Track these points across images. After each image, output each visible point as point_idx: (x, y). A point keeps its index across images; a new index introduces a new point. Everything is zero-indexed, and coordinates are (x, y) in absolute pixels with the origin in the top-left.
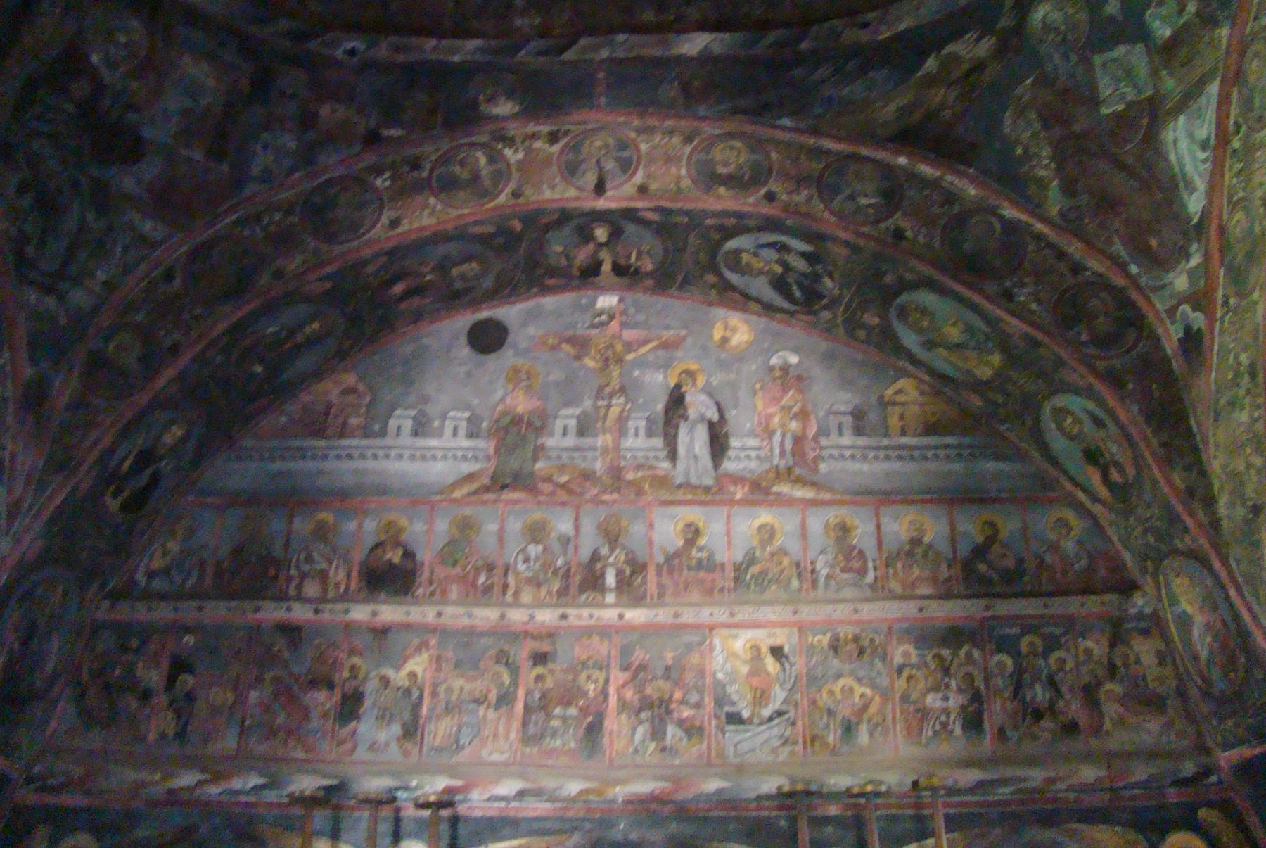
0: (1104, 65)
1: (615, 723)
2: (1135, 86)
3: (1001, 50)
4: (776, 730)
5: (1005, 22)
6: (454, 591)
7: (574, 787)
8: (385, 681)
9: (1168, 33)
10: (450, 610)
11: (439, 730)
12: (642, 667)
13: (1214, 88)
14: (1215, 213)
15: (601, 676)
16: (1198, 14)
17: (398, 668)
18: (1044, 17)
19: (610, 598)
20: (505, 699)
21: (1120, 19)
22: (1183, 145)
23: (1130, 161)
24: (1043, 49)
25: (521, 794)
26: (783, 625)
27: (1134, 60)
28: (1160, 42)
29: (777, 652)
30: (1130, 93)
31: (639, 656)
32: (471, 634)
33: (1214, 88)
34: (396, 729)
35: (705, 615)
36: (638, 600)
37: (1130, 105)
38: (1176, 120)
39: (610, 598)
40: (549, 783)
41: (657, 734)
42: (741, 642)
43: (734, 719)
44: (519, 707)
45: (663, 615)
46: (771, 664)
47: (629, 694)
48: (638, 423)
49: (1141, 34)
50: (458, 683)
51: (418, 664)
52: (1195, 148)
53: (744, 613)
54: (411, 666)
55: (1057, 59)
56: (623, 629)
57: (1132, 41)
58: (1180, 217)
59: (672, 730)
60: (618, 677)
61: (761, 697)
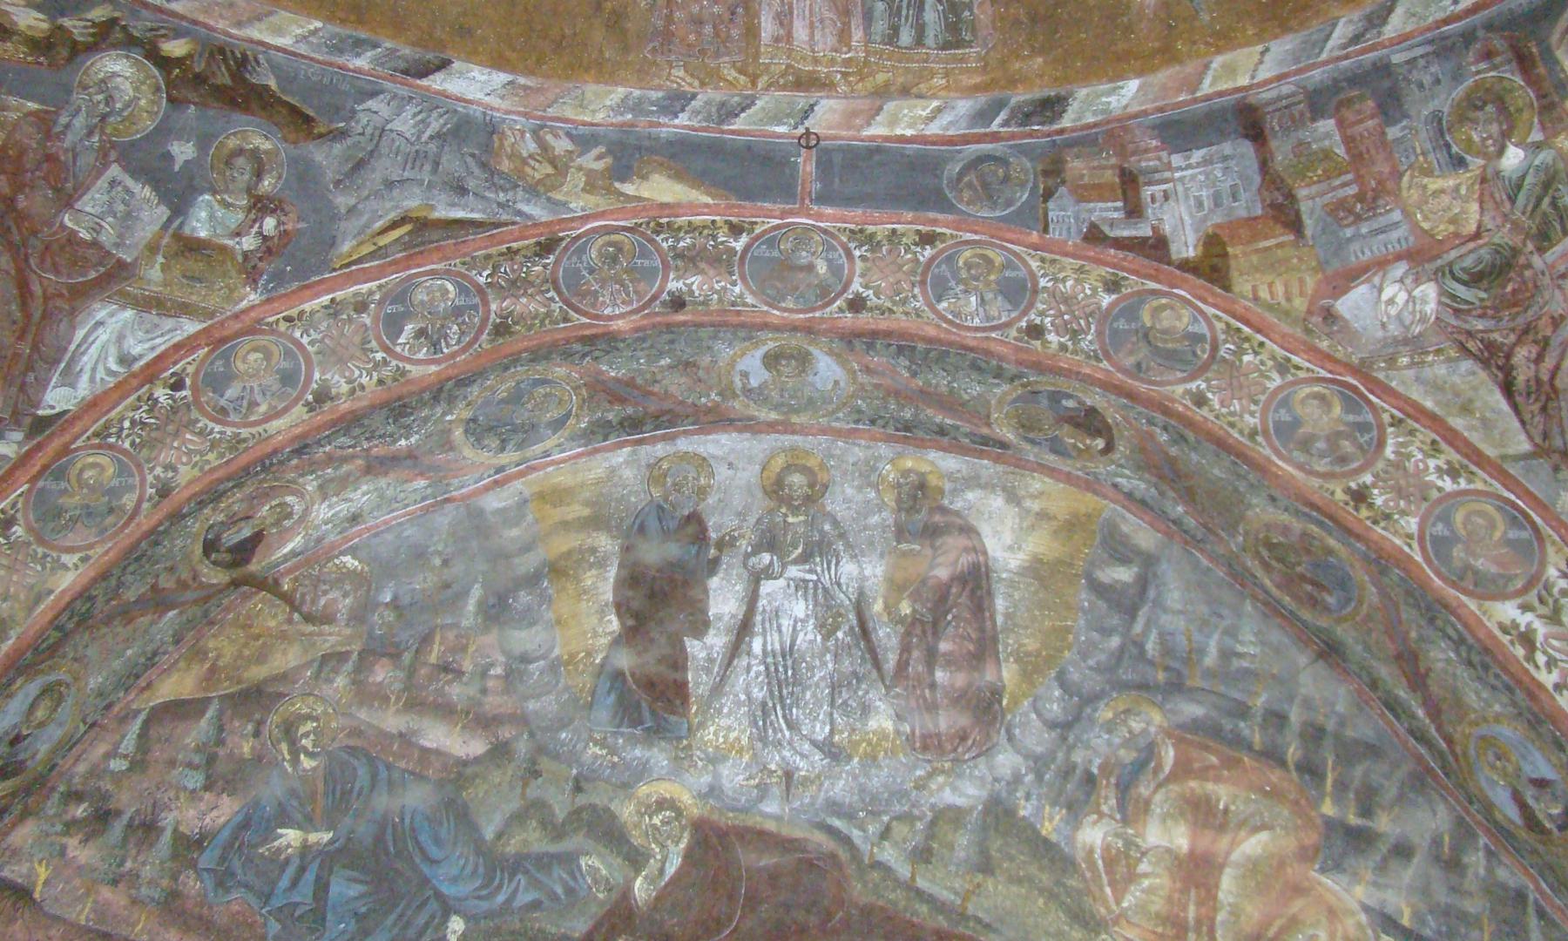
0: (113, 183)
2: (121, 236)
3: (42, 46)
5: (74, 25)
9: (203, 234)
13: (191, 327)
14: (76, 429)
16: (246, 255)
18: (115, 75)
21: (177, 168)
22: (103, 335)
23: (37, 289)
24: (79, 98)
27: (145, 215)
28: (187, 231)
30: (108, 237)
33: (191, 327)
37: (95, 244)
38: (124, 307)
49: (179, 205)
52: (113, 350)
55: (79, 122)
57: (164, 196)
58: (28, 394)
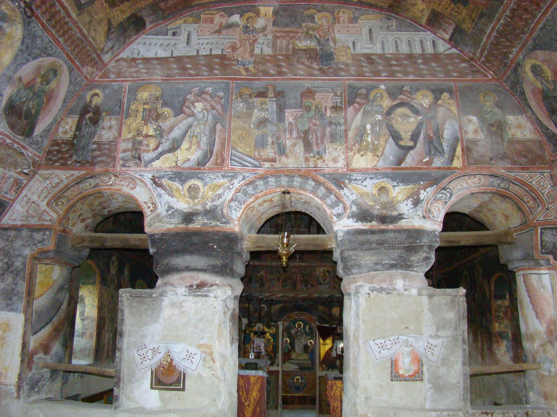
1: (299, 284)
4: (327, 286)
6: (268, 259)
7: (291, 295)
8: (257, 276)
10: (268, 263)
11: (267, 285)
12: (303, 274)
15: (296, 275)
17: (259, 273)
19: (298, 260)
20: (279, 279)
25: (282, 297)
26: (330, 266)
29: (328, 271)
31: (303, 272)
32: (272, 266)
34: (259, 284)
35: (315, 264)
36: (303, 261)
39: (298, 260)
40: (287, 295)
41: (306, 286)
42: (321, 270)
43: (320, 283)
44: (281, 281)
45: (307, 264)
46: (327, 274)
47: (301, 279)
48: (303, 225)
50: (270, 276)
51: (262, 273)
53: (322, 264)
54: (261, 273)
56: (300, 266)
59: (309, 285)
60: (299, 275)
61: (325, 280)
